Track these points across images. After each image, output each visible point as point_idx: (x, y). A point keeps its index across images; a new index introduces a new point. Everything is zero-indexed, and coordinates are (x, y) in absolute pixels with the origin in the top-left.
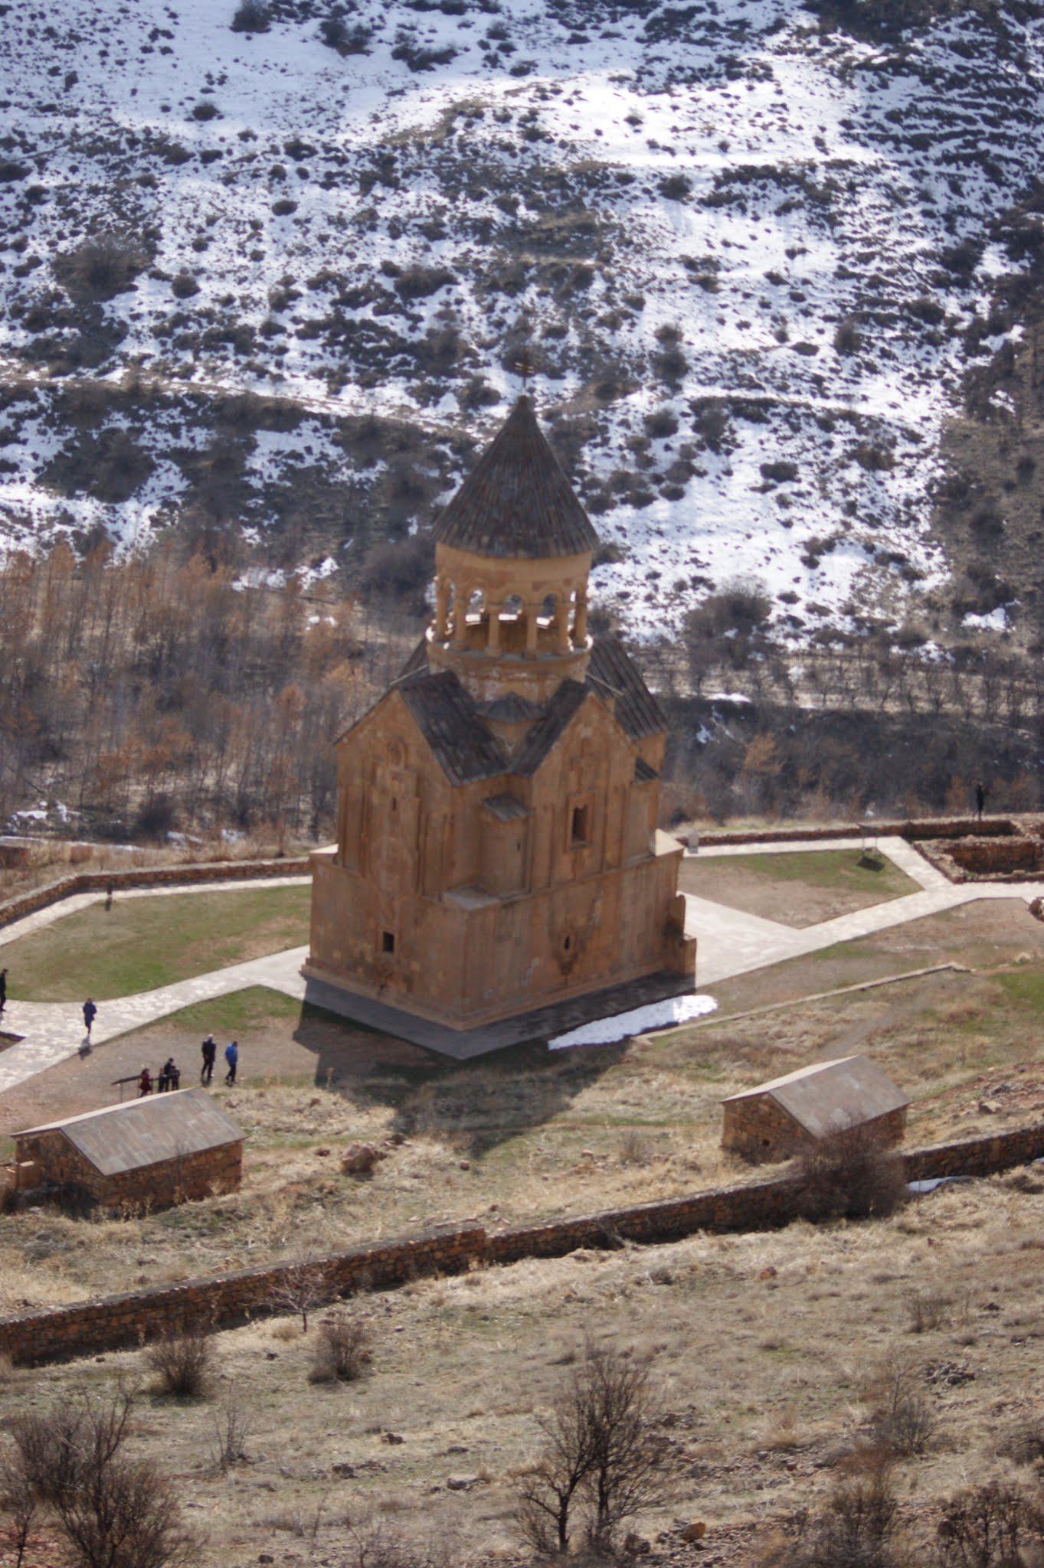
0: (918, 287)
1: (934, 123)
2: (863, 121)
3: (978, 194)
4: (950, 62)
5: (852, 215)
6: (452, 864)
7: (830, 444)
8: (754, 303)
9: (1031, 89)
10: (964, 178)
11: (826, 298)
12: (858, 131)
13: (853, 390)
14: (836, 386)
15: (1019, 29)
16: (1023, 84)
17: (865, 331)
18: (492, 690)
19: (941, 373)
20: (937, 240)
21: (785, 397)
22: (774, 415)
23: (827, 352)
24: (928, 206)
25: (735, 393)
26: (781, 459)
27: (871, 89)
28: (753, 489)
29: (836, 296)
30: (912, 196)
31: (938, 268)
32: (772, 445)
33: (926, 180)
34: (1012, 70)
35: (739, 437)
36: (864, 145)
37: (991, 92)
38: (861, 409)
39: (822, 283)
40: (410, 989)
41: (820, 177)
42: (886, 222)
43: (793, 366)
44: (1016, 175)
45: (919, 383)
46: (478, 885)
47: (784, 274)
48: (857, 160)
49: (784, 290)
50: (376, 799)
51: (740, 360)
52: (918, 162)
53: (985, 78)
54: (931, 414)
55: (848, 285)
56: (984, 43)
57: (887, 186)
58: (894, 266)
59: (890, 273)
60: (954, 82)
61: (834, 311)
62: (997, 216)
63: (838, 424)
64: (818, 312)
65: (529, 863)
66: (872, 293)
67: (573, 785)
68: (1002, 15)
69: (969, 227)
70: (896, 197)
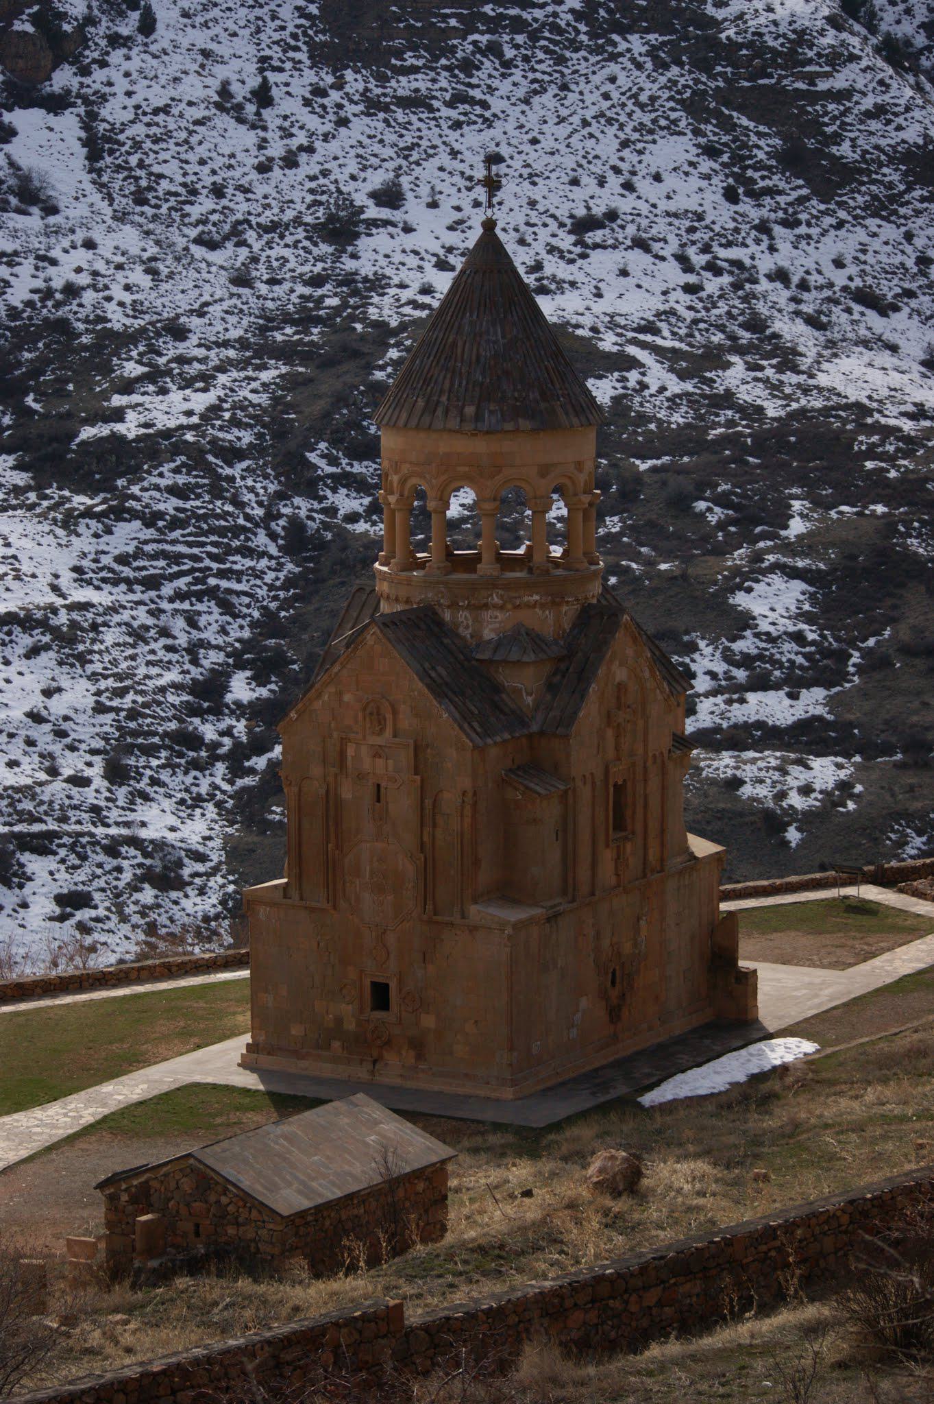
0: (174, 717)
1: (162, 563)
2: (94, 566)
3: (215, 627)
4: (169, 505)
5: (100, 652)
6: (477, 862)
7: (119, 869)
8: (19, 742)
9: (249, 525)
10: (199, 613)
11: (87, 731)
12: (91, 575)
13: (131, 817)
14: (114, 815)
15: (228, 471)
16: (241, 521)
17: (132, 761)
18: (492, 625)
19: (212, 796)
20: (183, 672)
21: (66, 827)
22: (59, 846)
23: (99, 783)
24: (169, 642)
25: (16, 829)
26: (74, 888)
27: (96, 536)
28: (51, 919)
29: (98, 729)
30: (152, 633)
31: (189, 698)
32: (62, 875)
33: (163, 617)
34: (229, 508)
35: (29, 869)
36: (98, 588)
37: (212, 531)
38: (144, 834)
39: (81, 718)
40: (420, 1057)
41: (63, 618)
42: (133, 658)
43: (69, 797)
44: (248, 606)
45: (193, 807)
46: (508, 890)
47: (44, 713)
48: (95, 600)
49: (47, 727)
50: (347, 794)
51: (17, 796)
52: (152, 601)
53: (204, 518)
54: (213, 833)
55: (108, 718)
56: (197, 485)
57: (127, 624)
58: (148, 698)
59: (145, 705)
60: (175, 524)
61: (99, 744)
62: (237, 645)
63: (123, 850)
64: (83, 746)
65: (569, 861)
66: (133, 725)
67: (611, 753)
68: (211, 458)
69: (212, 659)
70: (138, 635)
